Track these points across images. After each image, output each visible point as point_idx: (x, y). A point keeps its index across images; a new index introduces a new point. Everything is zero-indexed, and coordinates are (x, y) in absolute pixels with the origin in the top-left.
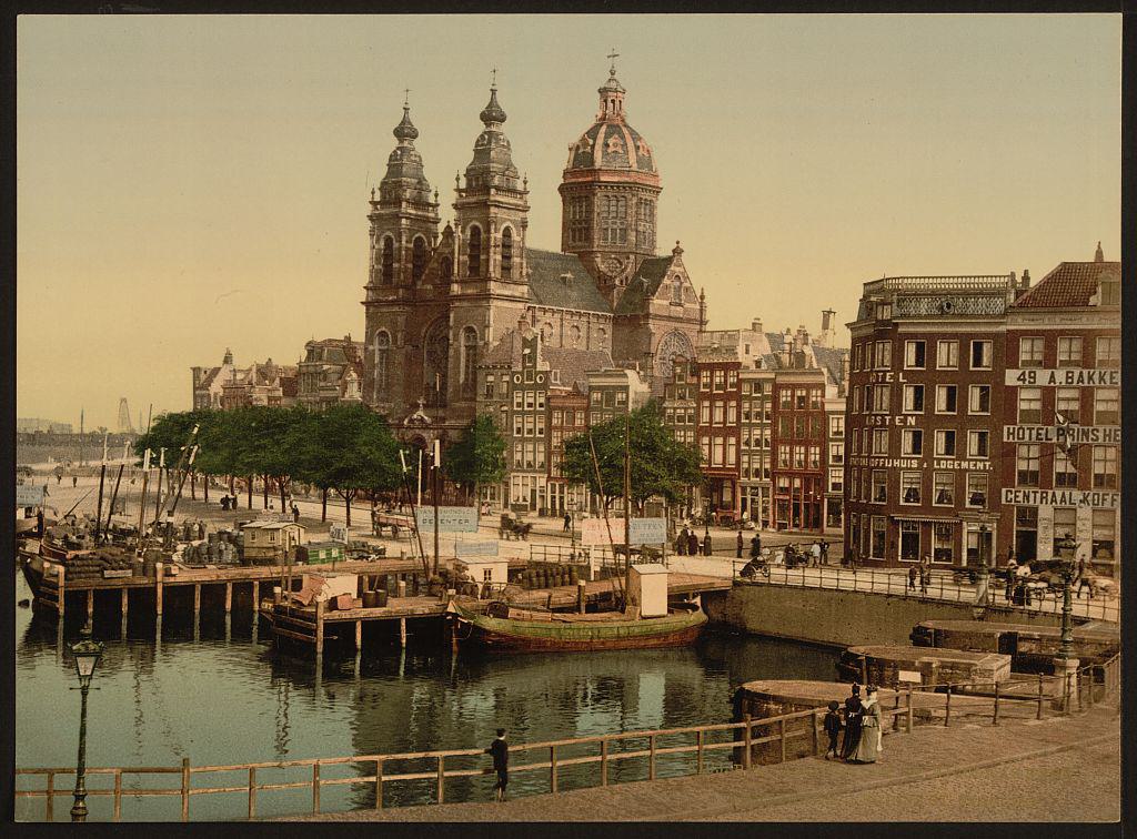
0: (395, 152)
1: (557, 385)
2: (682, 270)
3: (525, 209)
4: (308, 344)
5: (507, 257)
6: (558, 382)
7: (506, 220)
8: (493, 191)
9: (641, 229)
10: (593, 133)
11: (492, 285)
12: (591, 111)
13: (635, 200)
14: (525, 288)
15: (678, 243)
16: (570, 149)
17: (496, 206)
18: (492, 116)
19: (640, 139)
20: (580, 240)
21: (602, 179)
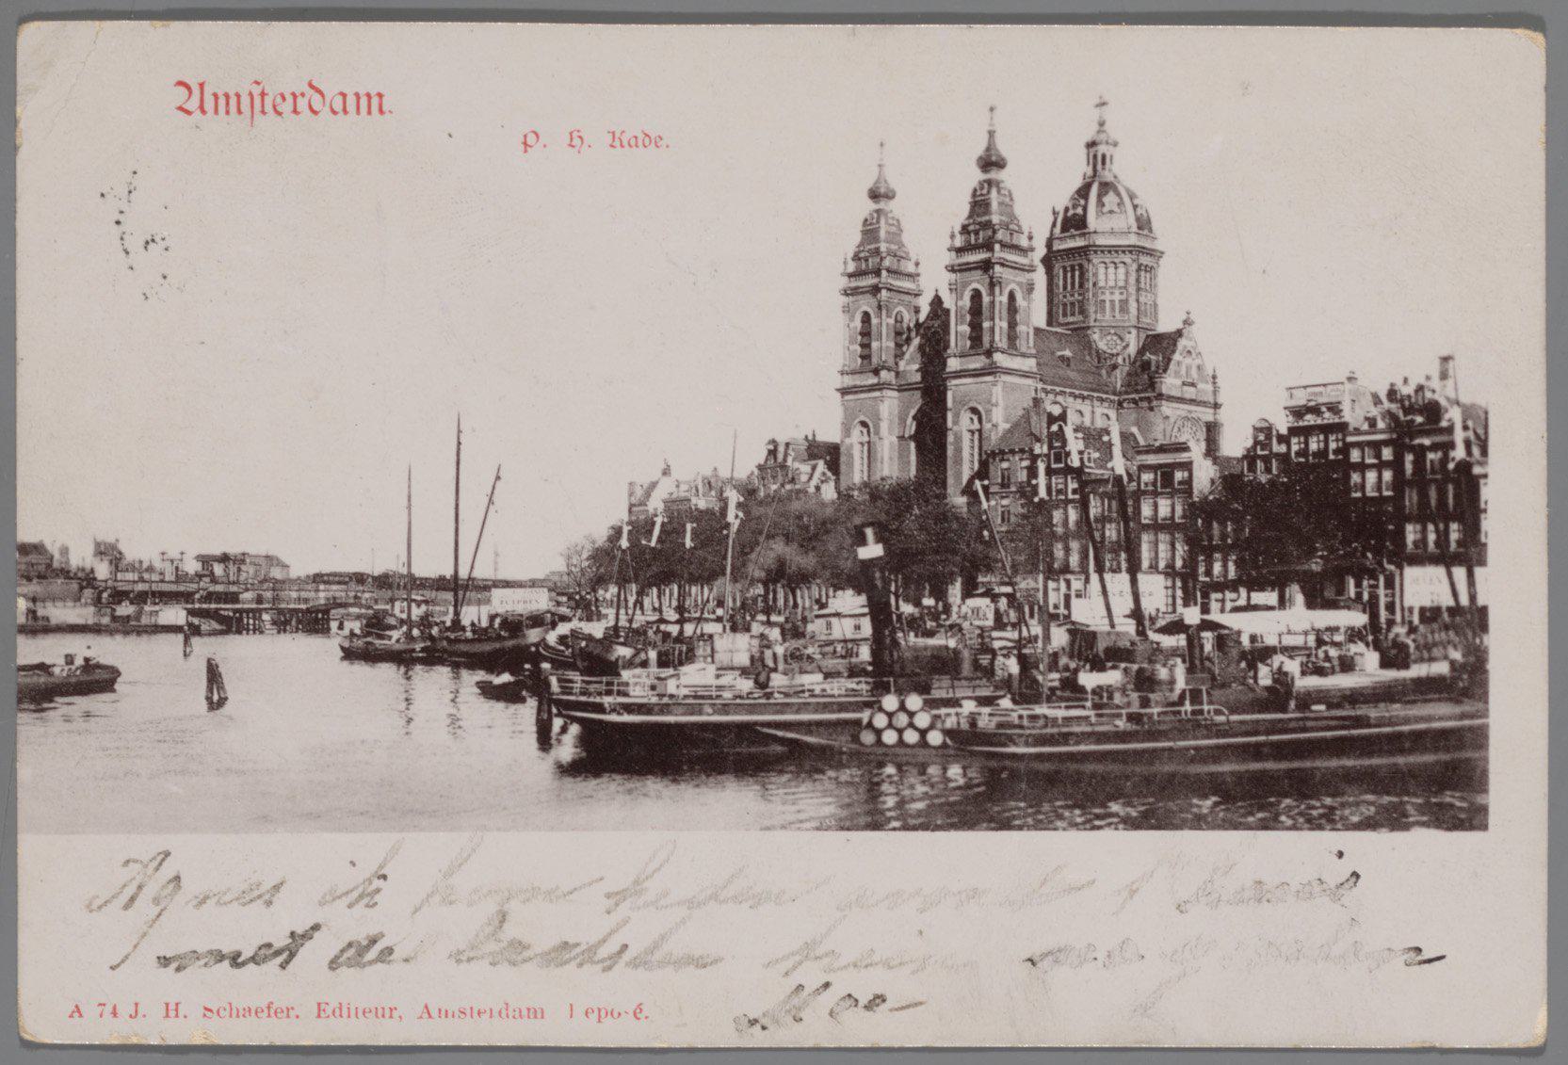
1: (1090, 468)
2: (1192, 343)
5: (1012, 325)
7: (1014, 281)
8: (997, 247)
9: (1142, 299)
10: (1083, 192)
12: (1077, 171)
13: (1135, 266)
18: (990, 162)
19: (1136, 197)
20: (1073, 314)
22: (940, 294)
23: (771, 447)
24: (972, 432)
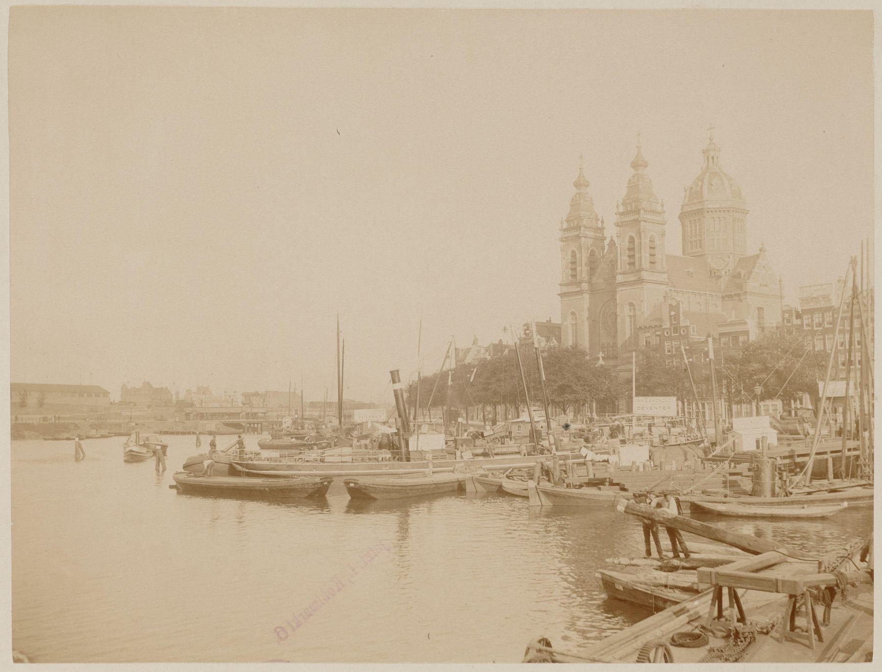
0: (575, 196)
1: (695, 335)
3: (663, 224)
4: (524, 325)
6: (695, 333)
8: (642, 212)
11: (645, 275)
14: (665, 276)
15: (763, 245)
16: (686, 191)
17: (645, 221)
21: (710, 206)
22: (613, 239)
23: (525, 328)
24: (630, 316)
